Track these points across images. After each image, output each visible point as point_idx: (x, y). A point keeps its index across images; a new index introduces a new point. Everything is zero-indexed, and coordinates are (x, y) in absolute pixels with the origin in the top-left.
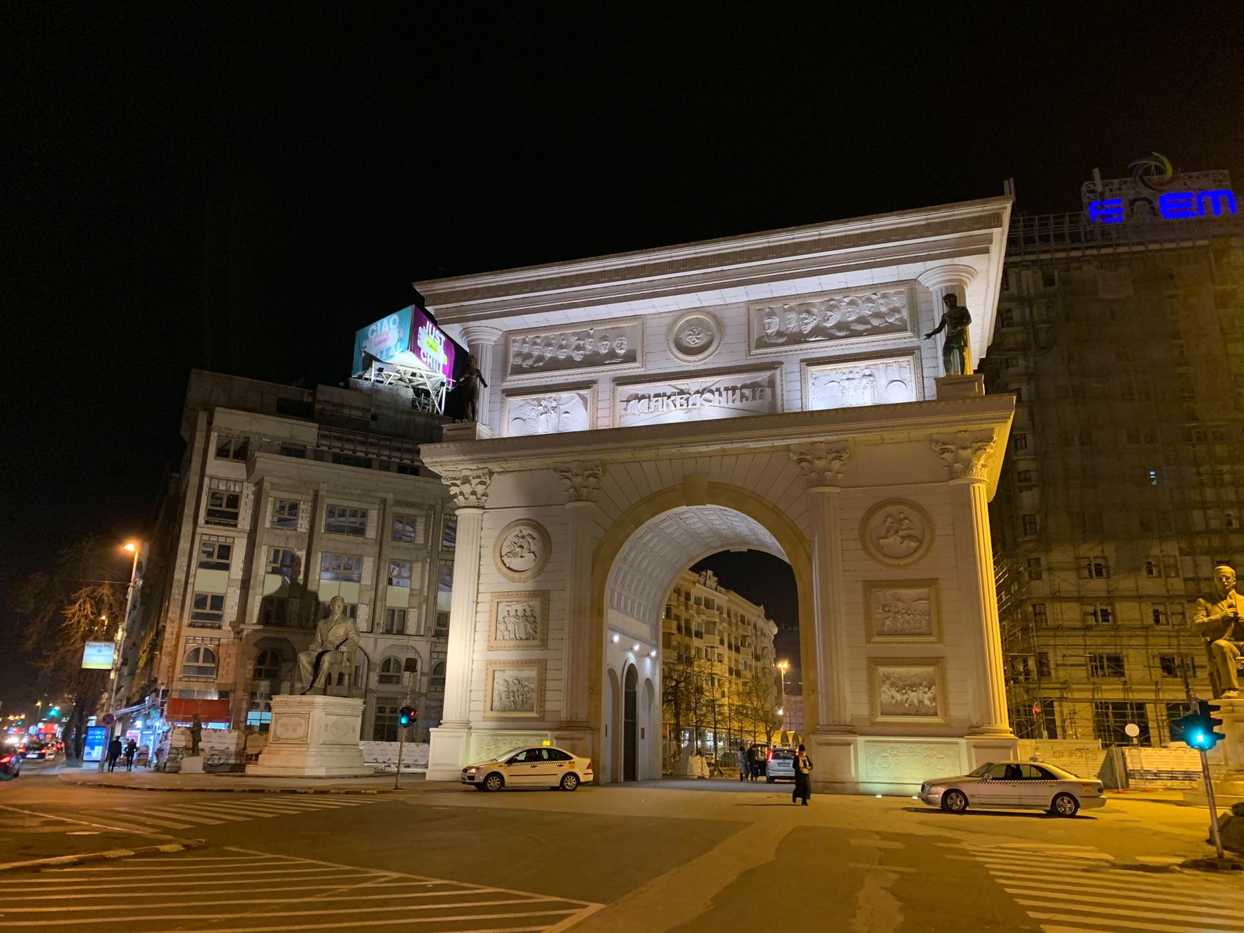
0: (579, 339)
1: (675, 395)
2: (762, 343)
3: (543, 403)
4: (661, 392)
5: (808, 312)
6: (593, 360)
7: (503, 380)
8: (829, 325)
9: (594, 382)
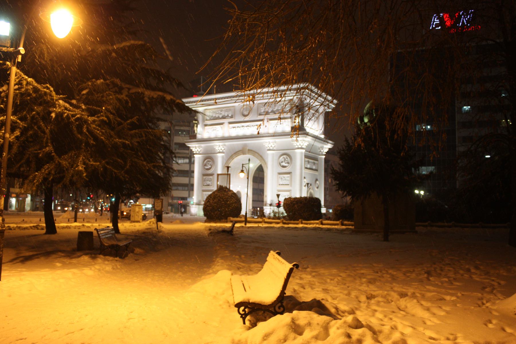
0: (221, 111)
3: (213, 128)
6: (224, 118)
7: (204, 122)
9: (224, 123)
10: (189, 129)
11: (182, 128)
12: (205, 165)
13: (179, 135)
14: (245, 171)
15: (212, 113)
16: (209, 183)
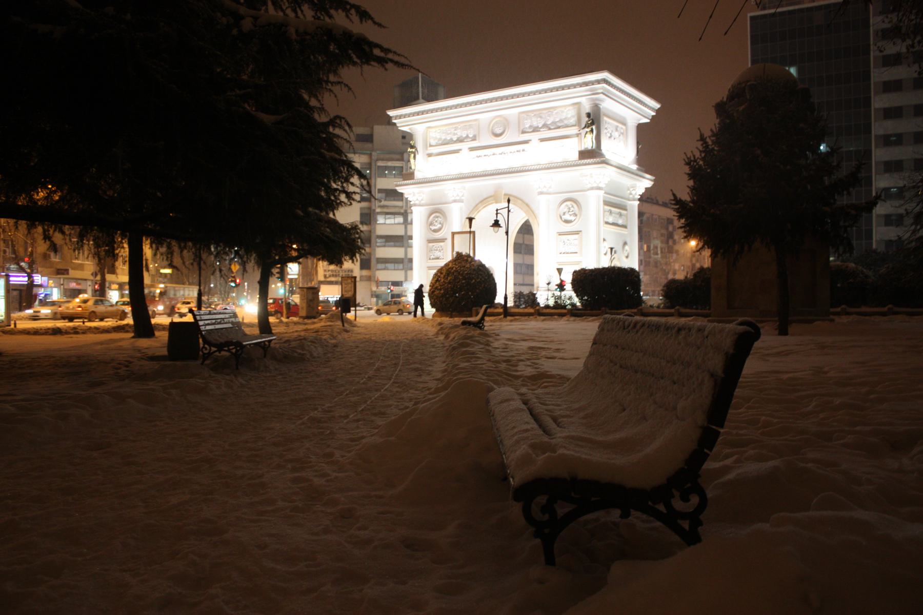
0: (455, 130)
1: (491, 155)
2: (523, 132)
4: (486, 154)
5: (541, 117)
6: (460, 140)
7: (427, 149)
8: (548, 123)
9: (461, 150)
10: (401, 165)
11: (390, 164)
12: (431, 224)
13: (385, 176)
14: (502, 222)
15: (440, 133)
16: (438, 254)
